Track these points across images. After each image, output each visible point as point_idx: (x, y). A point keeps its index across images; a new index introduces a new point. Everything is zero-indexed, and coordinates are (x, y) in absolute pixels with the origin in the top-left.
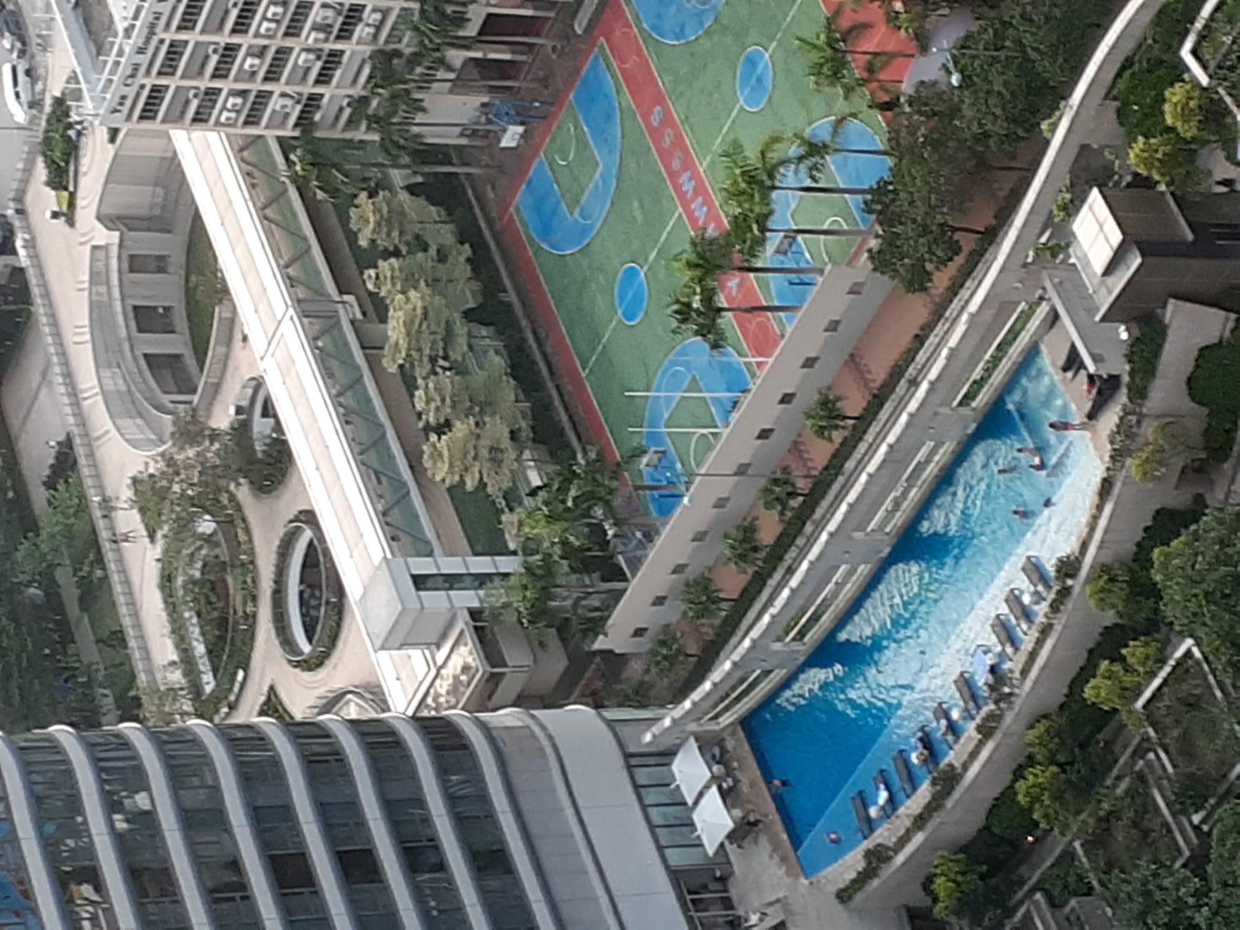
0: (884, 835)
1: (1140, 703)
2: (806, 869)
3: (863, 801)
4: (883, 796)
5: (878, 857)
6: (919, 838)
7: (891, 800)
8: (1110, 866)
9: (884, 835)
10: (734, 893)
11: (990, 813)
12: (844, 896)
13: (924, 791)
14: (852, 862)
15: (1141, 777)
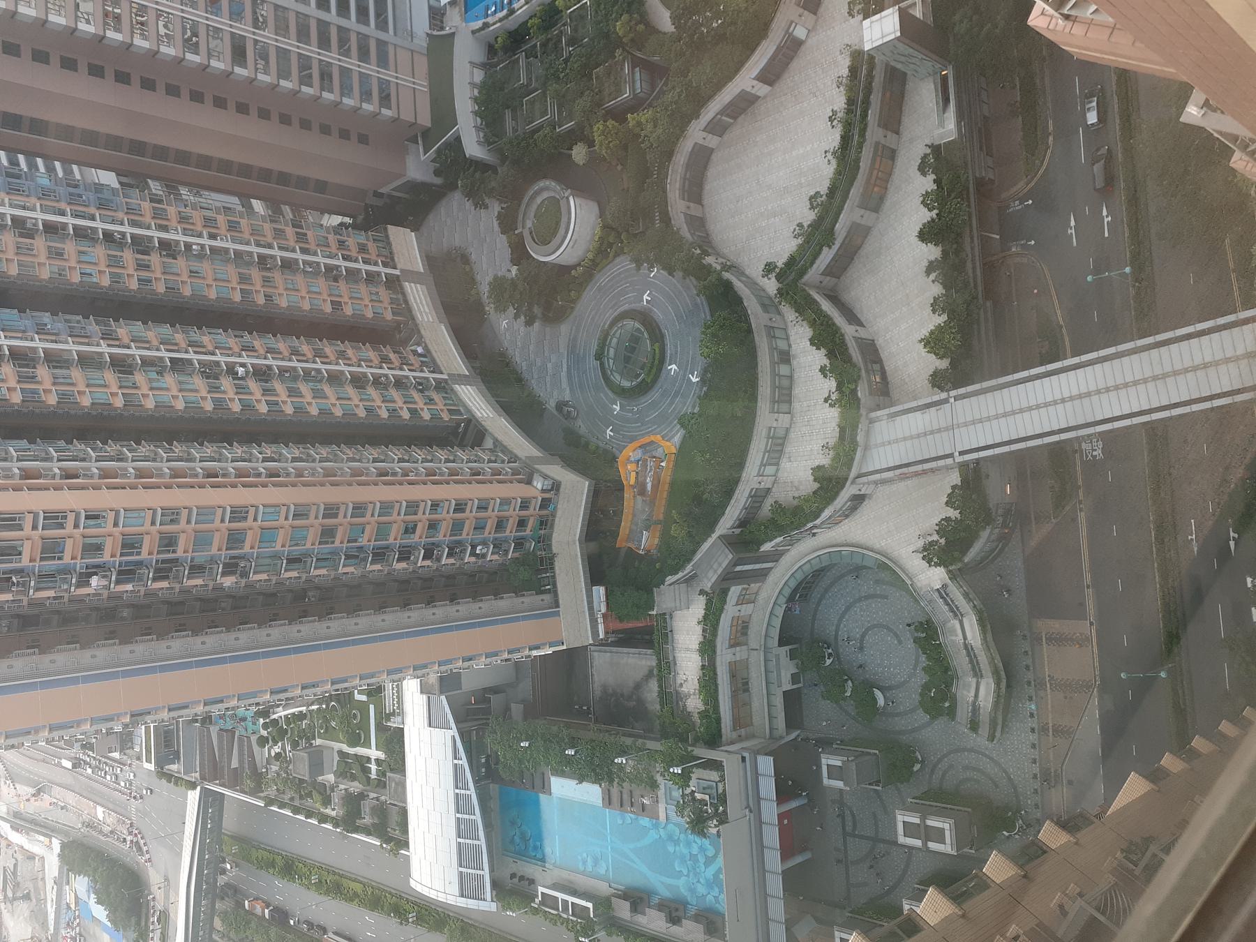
0: (490, 20)
1: (569, 11)
2: (466, 21)
3: (488, 8)
4: (494, 9)
5: (486, 25)
6: (498, 25)
7: (495, 10)
8: (544, 53)
9: (490, 20)
10: (444, 20)
11: (520, 25)
12: (474, 32)
13: (505, 12)
14: (479, 24)
15: (561, 32)
